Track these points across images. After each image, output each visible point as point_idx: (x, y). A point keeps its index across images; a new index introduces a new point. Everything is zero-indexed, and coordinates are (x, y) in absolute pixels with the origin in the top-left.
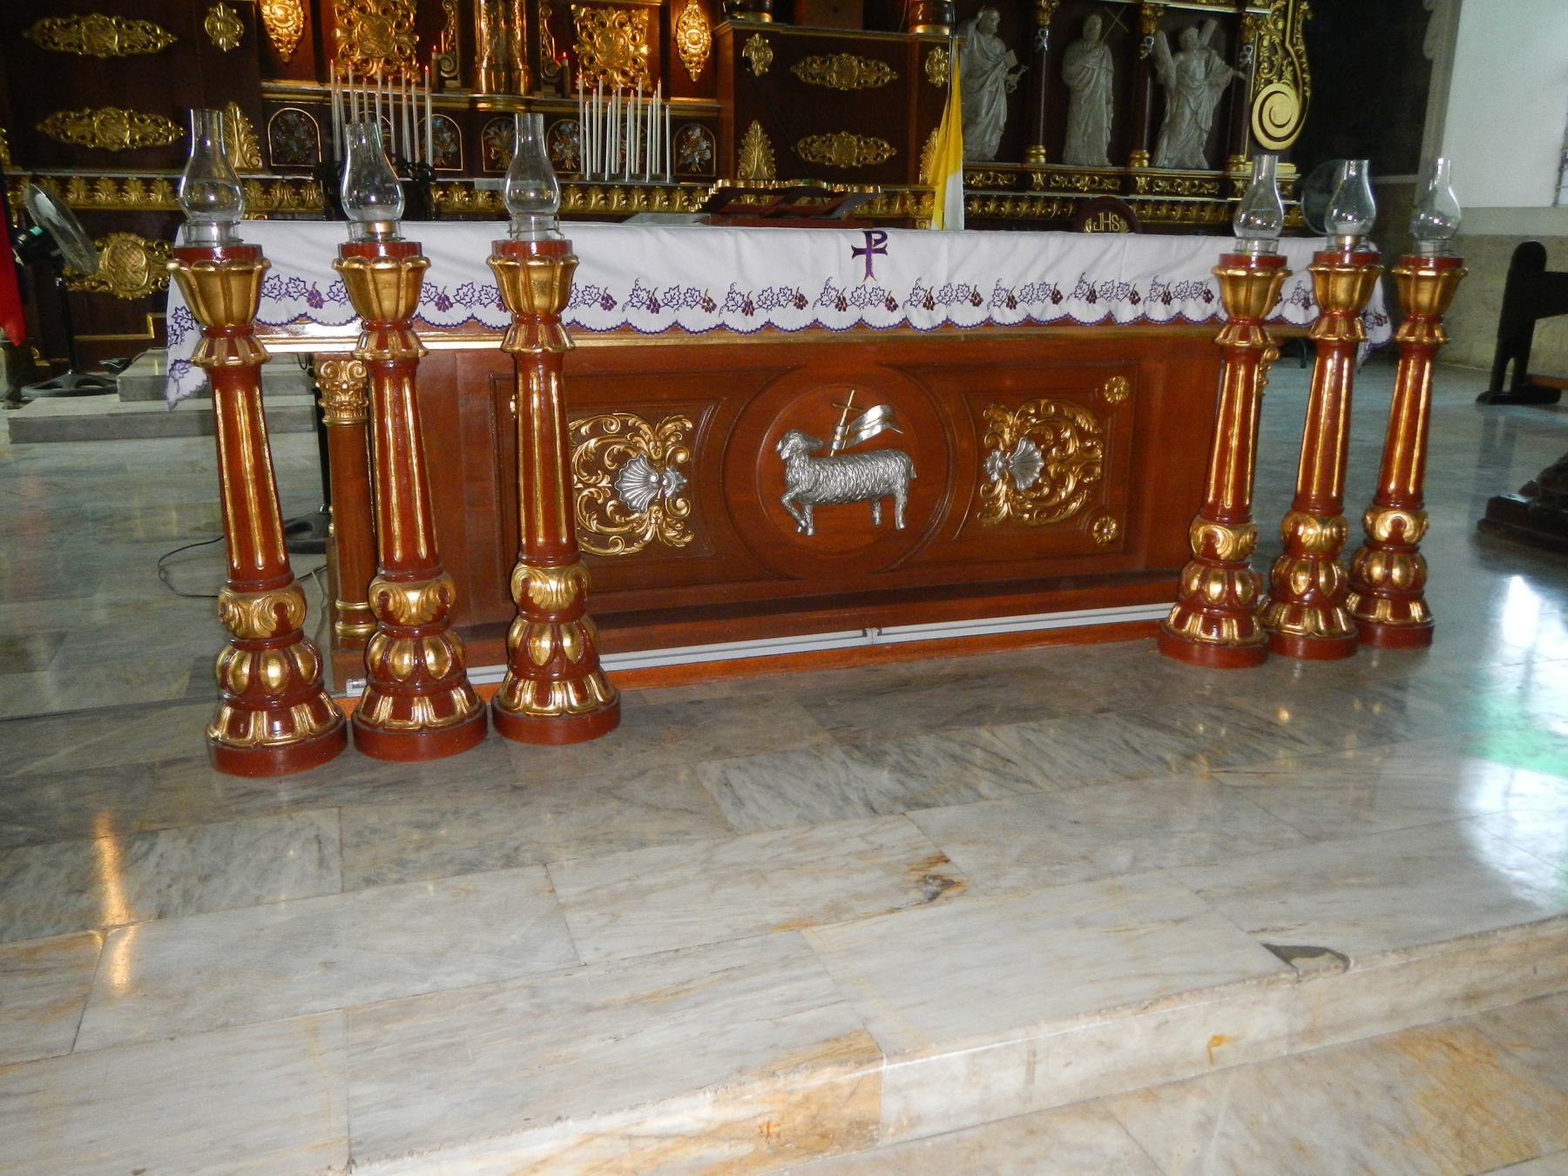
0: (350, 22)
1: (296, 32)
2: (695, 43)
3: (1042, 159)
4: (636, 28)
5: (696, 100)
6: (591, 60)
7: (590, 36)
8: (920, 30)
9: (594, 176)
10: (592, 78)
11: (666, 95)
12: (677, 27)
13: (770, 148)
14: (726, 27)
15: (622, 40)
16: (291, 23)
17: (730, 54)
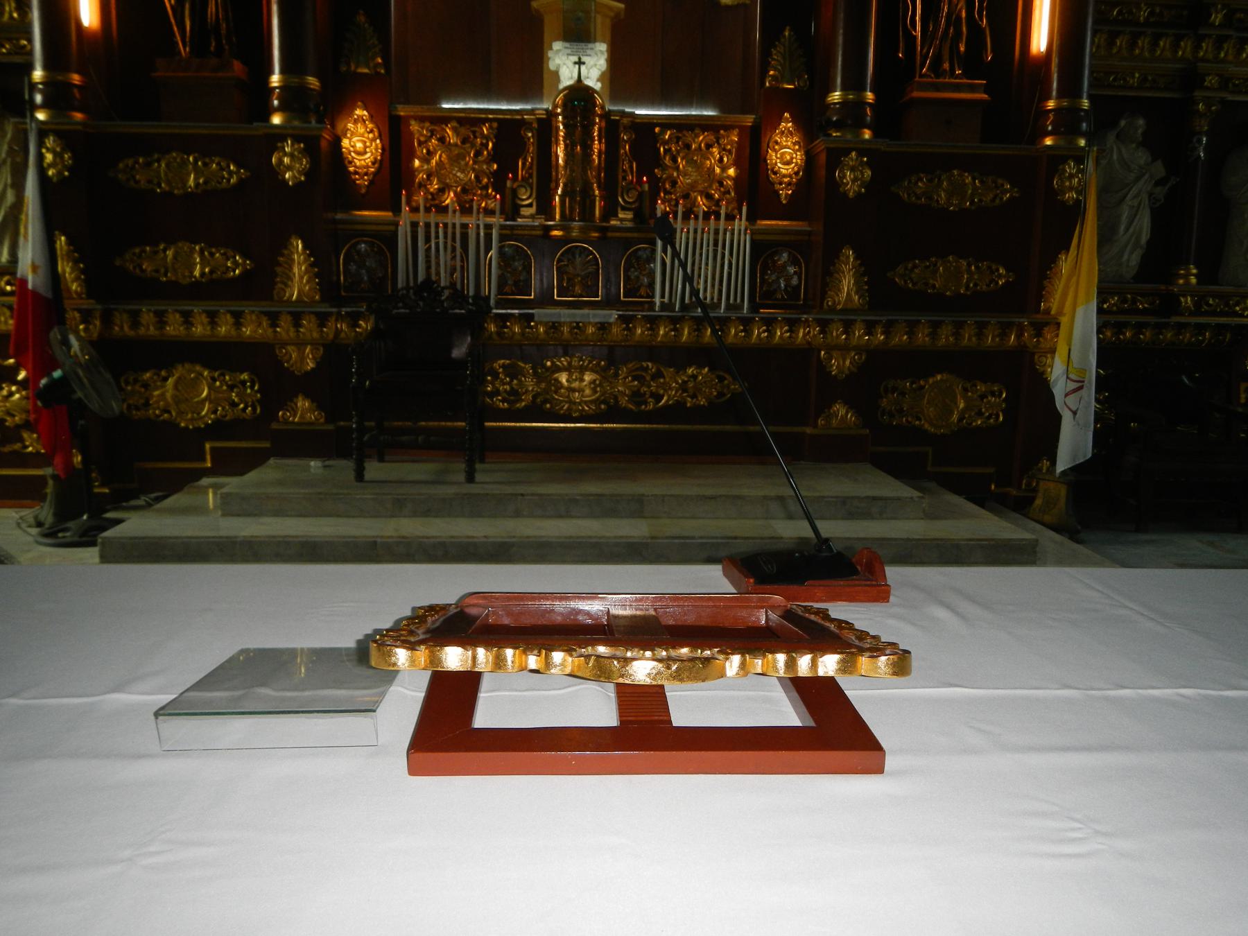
0: (429, 152)
1: (373, 163)
2: (788, 163)
3: (1193, 280)
4: (724, 149)
5: (785, 223)
6: (674, 183)
7: (674, 160)
8: (1048, 142)
9: (664, 307)
10: (673, 203)
11: (752, 218)
12: (768, 147)
13: (863, 275)
14: (820, 144)
15: (708, 162)
16: (368, 155)
17: (823, 172)
